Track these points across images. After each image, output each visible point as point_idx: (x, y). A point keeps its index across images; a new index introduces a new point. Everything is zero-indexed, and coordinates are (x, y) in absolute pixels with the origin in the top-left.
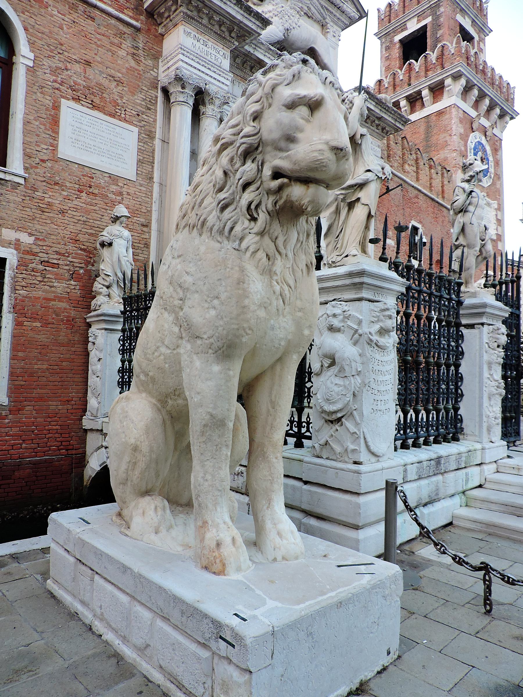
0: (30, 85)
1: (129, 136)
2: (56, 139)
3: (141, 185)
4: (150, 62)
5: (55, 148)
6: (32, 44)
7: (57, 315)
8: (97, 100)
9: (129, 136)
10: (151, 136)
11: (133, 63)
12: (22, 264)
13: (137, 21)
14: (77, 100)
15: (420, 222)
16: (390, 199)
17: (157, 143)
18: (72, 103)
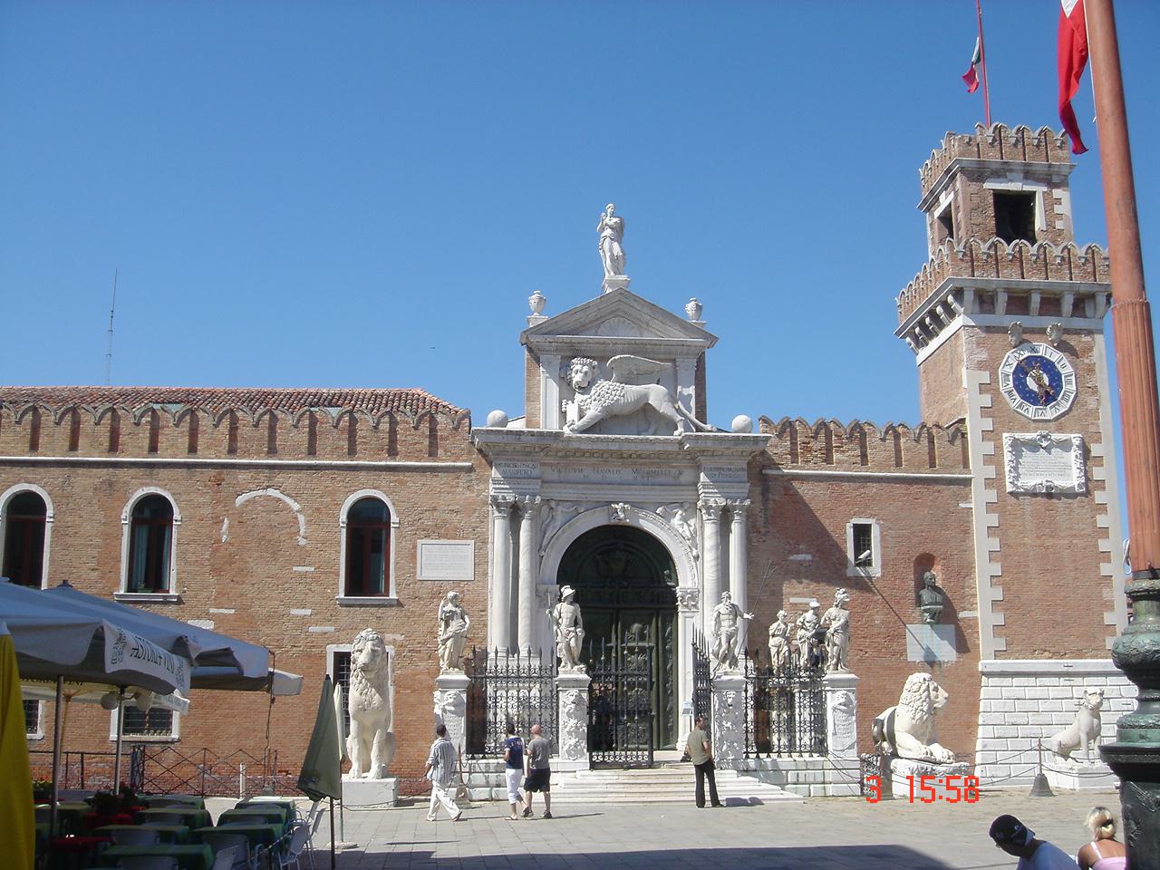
0: (397, 538)
1: (468, 549)
2: (415, 568)
3: (479, 581)
4: (482, 487)
5: (415, 573)
7: (421, 684)
8: (442, 531)
9: (468, 549)
10: (485, 542)
11: (468, 494)
12: (398, 654)
13: (470, 461)
14: (427, 536)
15: (871, 516)
17: (489, 545)
18: (424, 541)
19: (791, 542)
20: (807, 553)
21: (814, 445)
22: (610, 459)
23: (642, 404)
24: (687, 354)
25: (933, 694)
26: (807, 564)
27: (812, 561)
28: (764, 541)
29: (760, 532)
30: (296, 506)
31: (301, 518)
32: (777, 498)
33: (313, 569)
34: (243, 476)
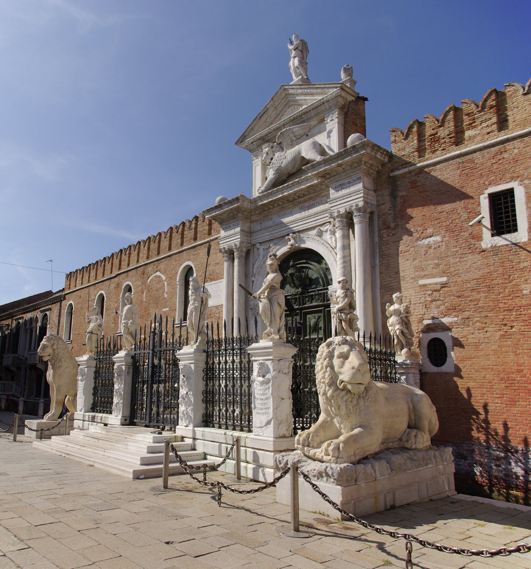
6: (196, 270)
15: (512, 179)
16: (428, 193)
19: (419, 229)
20: (436, 235)
21: (443, 132)
22: (284, 205)
23: (299, 162)
24: (330, 107)
25: (336, 362)
26: (435, 246)
27: (442, 242)
28: (393, 235)
29: (389, 228)
30: (164, 278)
31: (166, 283)
32: (404, 193)
33: (167, 309)
34: (150, 268)
